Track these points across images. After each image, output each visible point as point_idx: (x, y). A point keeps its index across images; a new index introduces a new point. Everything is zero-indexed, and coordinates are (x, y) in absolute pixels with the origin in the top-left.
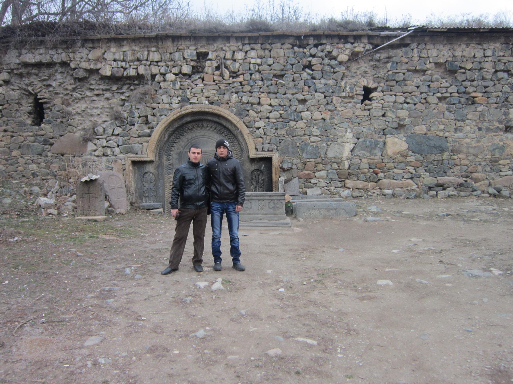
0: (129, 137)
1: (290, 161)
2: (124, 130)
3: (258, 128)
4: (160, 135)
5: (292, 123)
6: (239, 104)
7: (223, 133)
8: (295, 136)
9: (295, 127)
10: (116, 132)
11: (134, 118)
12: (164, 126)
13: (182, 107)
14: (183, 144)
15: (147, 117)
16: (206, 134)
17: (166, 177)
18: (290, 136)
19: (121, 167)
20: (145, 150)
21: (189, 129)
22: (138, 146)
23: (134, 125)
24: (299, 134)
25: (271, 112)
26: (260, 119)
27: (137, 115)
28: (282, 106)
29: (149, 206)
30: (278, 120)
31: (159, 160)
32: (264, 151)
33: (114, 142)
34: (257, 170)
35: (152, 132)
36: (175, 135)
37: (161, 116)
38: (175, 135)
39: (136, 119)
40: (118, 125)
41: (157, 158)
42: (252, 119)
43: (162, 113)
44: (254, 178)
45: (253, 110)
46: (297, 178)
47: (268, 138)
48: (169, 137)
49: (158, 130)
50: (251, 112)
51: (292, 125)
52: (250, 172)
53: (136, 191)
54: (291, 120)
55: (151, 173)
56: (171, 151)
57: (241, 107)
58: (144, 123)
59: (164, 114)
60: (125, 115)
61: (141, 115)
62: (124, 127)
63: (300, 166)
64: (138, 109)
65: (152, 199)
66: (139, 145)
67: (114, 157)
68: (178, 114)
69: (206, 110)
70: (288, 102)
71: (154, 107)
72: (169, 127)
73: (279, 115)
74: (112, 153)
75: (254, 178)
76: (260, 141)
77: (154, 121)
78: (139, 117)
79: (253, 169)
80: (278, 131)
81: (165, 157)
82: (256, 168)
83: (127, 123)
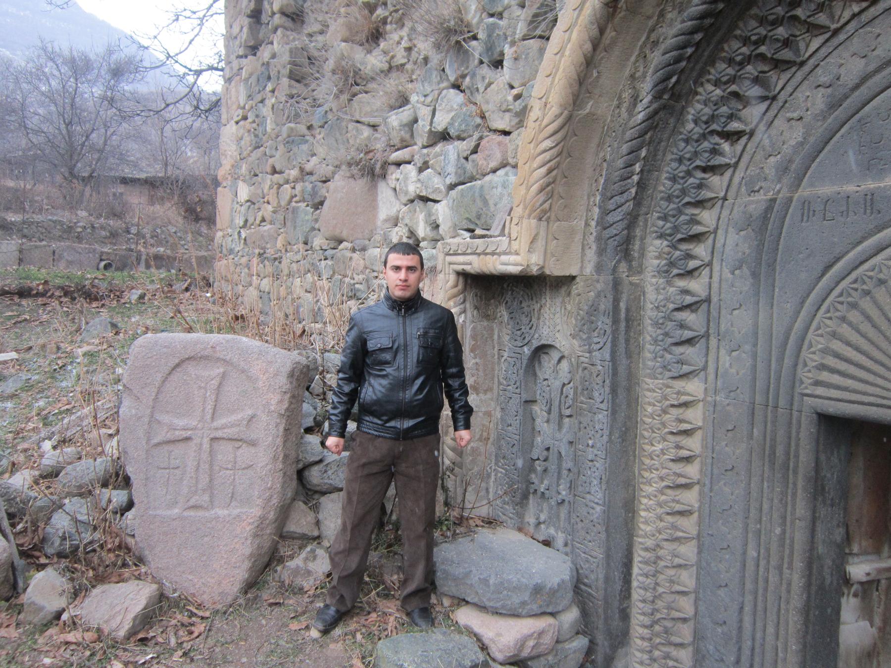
14: (795, 135)
38: (722, 69)
56: (700, 204)
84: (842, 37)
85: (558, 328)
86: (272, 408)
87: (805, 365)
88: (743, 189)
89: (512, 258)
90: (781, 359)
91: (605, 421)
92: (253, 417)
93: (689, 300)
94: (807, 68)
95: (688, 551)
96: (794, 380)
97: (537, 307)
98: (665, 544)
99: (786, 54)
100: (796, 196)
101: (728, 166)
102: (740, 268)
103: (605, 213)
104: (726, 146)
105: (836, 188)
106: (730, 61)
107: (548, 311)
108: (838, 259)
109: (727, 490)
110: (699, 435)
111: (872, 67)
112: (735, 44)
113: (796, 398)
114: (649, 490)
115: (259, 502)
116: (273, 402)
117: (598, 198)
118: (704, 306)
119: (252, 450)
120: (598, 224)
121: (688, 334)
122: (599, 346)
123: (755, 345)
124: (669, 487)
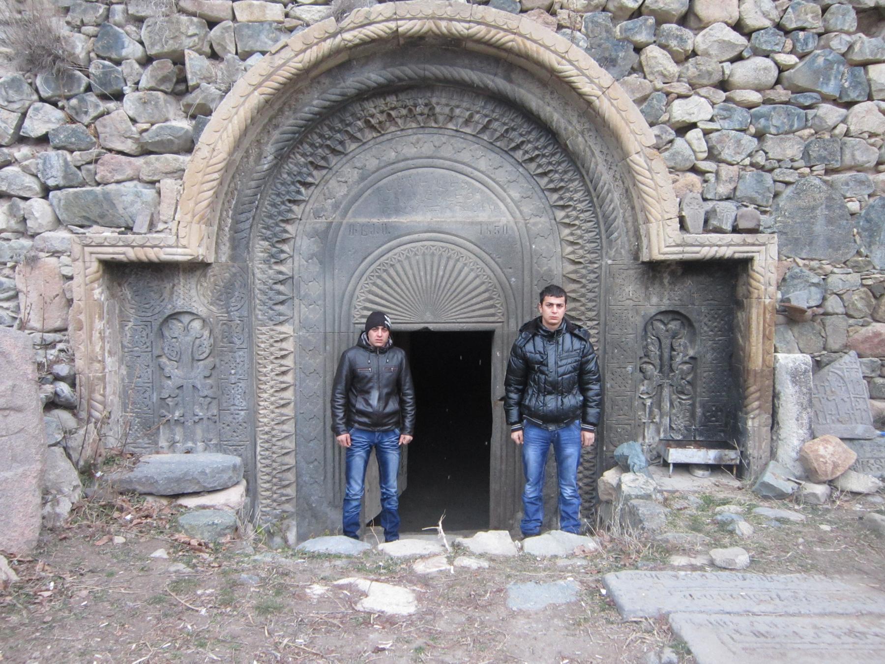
0: (95, 151)
1: (815, 280)
2: (73, 121)
3: (683, 129)
4: (238, 144)
5: (830, 113)
6: (602, 18)
7: (517, 147)
8: (836, 171)
9: (842, 128)
10: (35, 127)
11: (118, 63)
12: (256, 99)
13: (339, 16)
14: (343, 190)
15: (179, 60)
16: (447, 151)
17: (264, 335)
18: (819, 169)
19: (57, 287)
20: (166, 211)
21: (367, 122)
22: (138, 195)
23: (119, 96)
24: (861, 158)
25: (739, 58)
26: (693, 86)
27: (132, 50)
28: (787, 32)
29: (178, 480)
30: (771, 94)
31: (233, 258)
32: (718, 230)
33: (25, 169)
34: (674, 314)
35: (199, 129)
36: (307, 148)
37: (245, 56)
38: (307, 148)
39: (130, 68)
40: (46, 93)
41: (226, 249)
42: (659, 85)
43: (251, 44)
44: (654, 349)
45: (663, 47)
46: (853, 353)
47: (724, 169)
48: (282, 157)
49: (229, 119)
50: (653, 52)
51: (831, 122)
52: (639, 321)
53: (124, 395)
54: (826, 99)
55: (195, 316)
56: (287, 221)
57: (608, 31)
58: (168, 87)
59: (258, 46)
60: (80, 46)
61: (152, 52)
62: (74, 102)
63: (858, 300)
64: (139, 21)
65: (199, 431)
66: (140, 187)
67: (26, 242)
68: (327, 46)
69: (460, 28)
70: (815, 17)
71: (215, 14)
72: (281, 110)
73: (775, 73)
74: (13, 224)
75: (654, 349)
76: (690, 188)
77: (209, 80)
78: (146, 61)
79: (653, 311)
80: (770, 143)
81: (260, 247)
82: (666, 305)
83: (89, 89)
84: (367, 146)
85: (194, 299)
86: (30, 377)
87: (355, 308)
88: (312, 215)
89: (180, 250)
90: (341, 307)
91: (246, 355)
92: (14, 386)
93: (281, 277)
94: (348, 157)
95: (289, 427)
96: (349, 316)
97: (169, 286)
98: (276, 427)
99: (339, 148)
100: (345, 222)
101: (304, 201)
102: (311, 258)
103: (236, 222)
104: (303, 190)
105: (367, 220)
106: (312, 145)
107: (182, 289)
108: (369, 255)
109: (311, 384)
110: (291, 357)
111: (382, 164)
112: (315, 137)
113: (352, 326)
114: (265, 395)
115: (38, 457)
116: (29, 371)
117: (231, 213)
118: (290, 281)
119: (20, 415)
120: (231, 229)
121: (282, 298)
122: (236, 308)
123: (325, 300)
124: (276, 391)
